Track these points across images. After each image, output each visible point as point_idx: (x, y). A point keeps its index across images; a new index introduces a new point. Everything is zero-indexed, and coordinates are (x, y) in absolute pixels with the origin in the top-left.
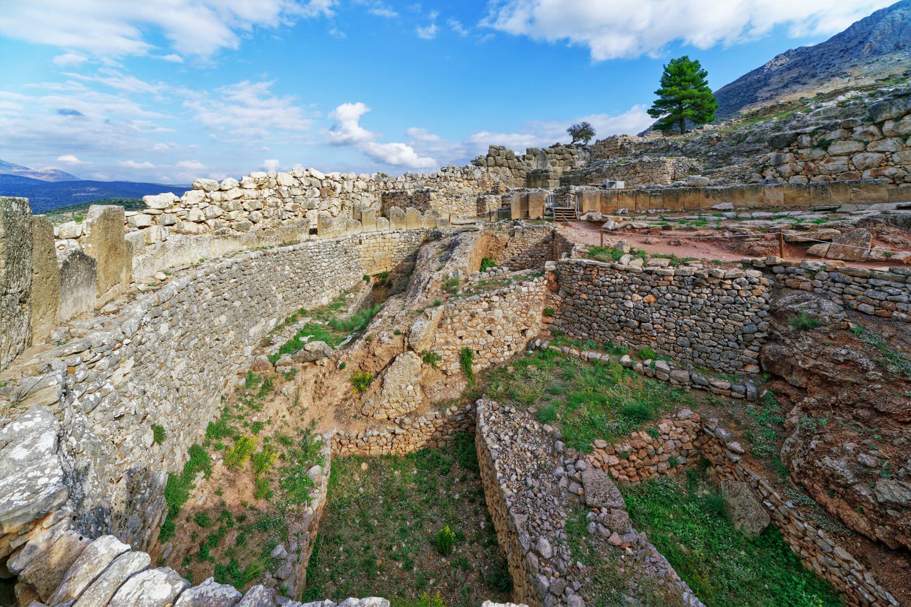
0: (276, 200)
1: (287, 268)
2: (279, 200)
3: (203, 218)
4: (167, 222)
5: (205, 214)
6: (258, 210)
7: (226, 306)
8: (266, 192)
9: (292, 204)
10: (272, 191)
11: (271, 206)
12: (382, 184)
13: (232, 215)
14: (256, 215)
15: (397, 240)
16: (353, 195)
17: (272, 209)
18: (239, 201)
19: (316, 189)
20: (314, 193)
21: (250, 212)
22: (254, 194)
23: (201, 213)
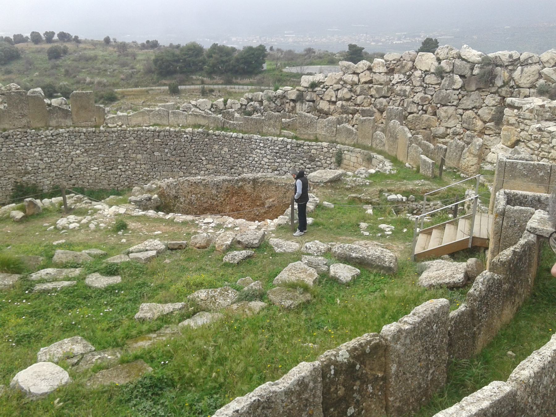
0: (404, 87)
1: (226, 149)
2: (408, 88)
3: (334, 99)
4: (308, 98)
5: (336, 96)
6: (385, 97)
7: (146, 151)
8: (397, 77)
9: (421, 95)
10: (402, 76)
11: (398, 95)
13: (359, 99)
14: (381, 103)
17: (398, 98)
18: (366, 86)
19: (457, 77)
20: (453, 82)
21: (376, 98)
22: (383, 78)
23: (333, 93)
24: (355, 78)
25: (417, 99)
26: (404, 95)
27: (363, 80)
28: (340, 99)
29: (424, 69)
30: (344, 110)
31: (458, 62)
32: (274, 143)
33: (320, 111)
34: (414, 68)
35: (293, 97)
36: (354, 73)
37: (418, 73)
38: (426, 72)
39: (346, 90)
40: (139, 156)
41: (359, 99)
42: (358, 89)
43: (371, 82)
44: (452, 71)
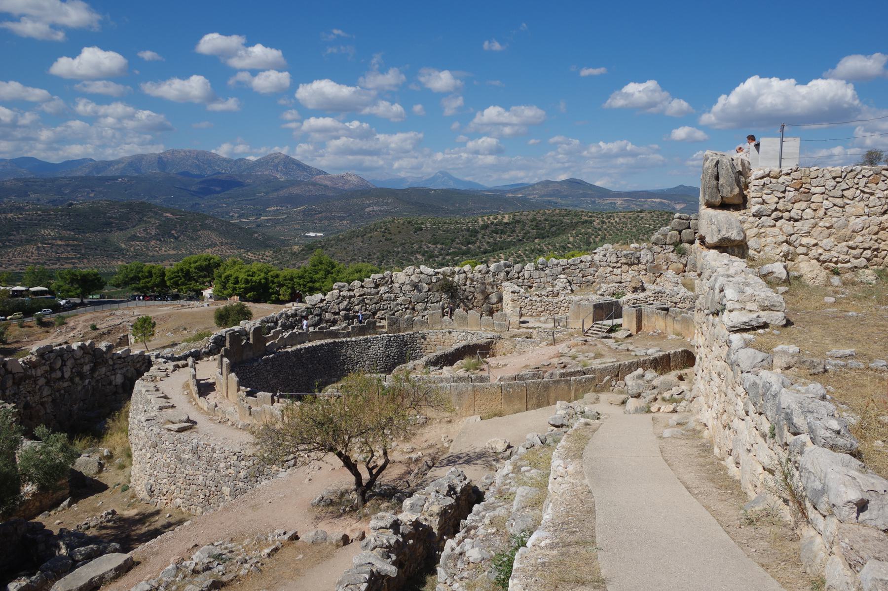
6: (376, 303)
8: (382, 289)
9: (403, 298)
12: (502, 274)
15: (456, 338)
16: (464, 288)
24: (351, 293)
25: (399, 301)
26: (389, 300)
27: (357, 294)
28: (343, 310)
29: (400, 282)
30: (346, 317)
31: (422, 276)
32: (382, 339)
33: (327, 322)
34: (392, 282)
35: (304, 314)
36: (350, 290)
37: (396, 285)
38: (403, 284)
39: (346, 303)
40: (300, 371)
41: (357, 308)
42: (356, 300)
43: (364, 294)
44: (420, 281)
